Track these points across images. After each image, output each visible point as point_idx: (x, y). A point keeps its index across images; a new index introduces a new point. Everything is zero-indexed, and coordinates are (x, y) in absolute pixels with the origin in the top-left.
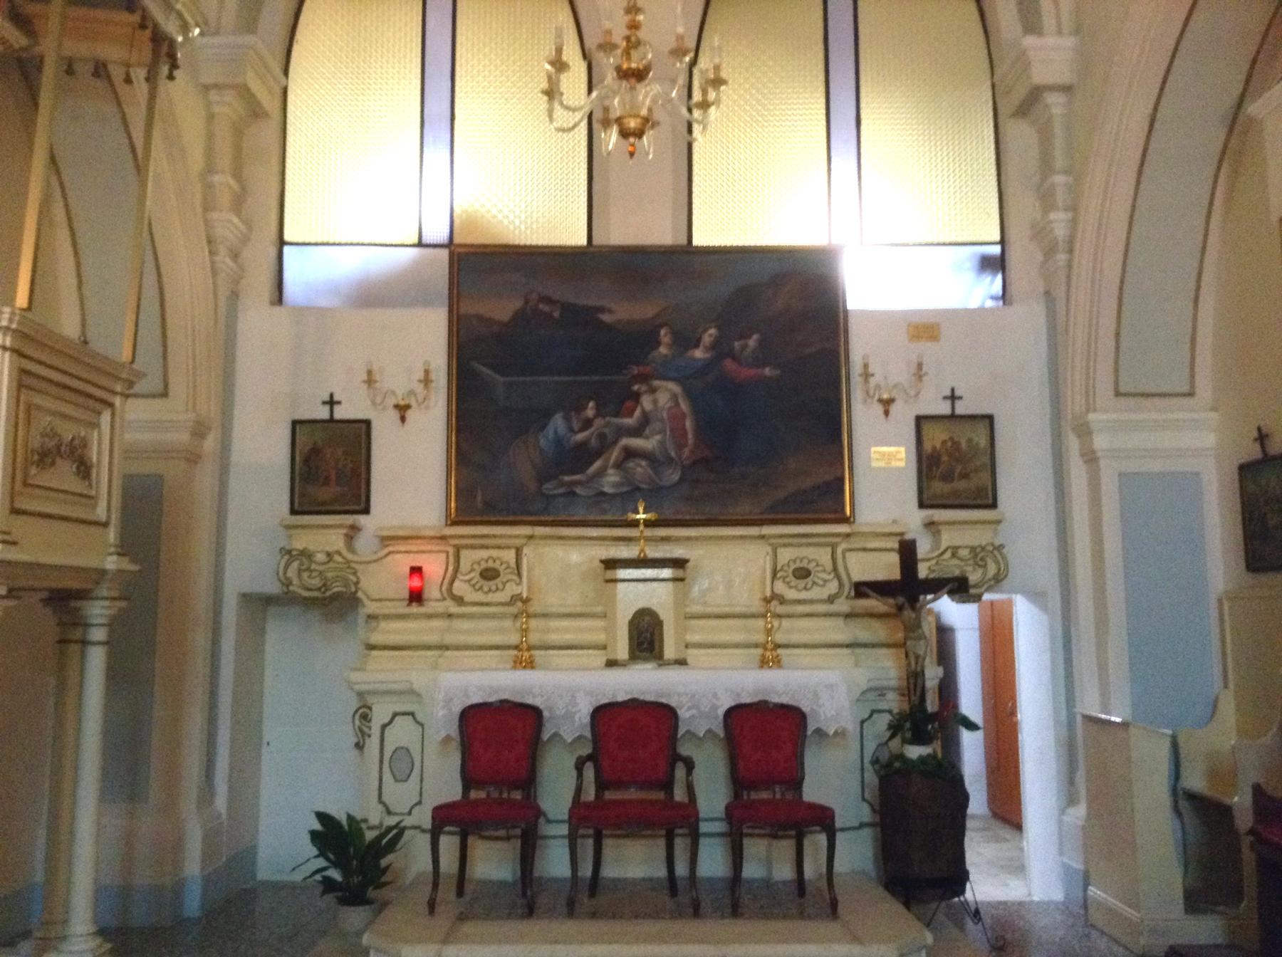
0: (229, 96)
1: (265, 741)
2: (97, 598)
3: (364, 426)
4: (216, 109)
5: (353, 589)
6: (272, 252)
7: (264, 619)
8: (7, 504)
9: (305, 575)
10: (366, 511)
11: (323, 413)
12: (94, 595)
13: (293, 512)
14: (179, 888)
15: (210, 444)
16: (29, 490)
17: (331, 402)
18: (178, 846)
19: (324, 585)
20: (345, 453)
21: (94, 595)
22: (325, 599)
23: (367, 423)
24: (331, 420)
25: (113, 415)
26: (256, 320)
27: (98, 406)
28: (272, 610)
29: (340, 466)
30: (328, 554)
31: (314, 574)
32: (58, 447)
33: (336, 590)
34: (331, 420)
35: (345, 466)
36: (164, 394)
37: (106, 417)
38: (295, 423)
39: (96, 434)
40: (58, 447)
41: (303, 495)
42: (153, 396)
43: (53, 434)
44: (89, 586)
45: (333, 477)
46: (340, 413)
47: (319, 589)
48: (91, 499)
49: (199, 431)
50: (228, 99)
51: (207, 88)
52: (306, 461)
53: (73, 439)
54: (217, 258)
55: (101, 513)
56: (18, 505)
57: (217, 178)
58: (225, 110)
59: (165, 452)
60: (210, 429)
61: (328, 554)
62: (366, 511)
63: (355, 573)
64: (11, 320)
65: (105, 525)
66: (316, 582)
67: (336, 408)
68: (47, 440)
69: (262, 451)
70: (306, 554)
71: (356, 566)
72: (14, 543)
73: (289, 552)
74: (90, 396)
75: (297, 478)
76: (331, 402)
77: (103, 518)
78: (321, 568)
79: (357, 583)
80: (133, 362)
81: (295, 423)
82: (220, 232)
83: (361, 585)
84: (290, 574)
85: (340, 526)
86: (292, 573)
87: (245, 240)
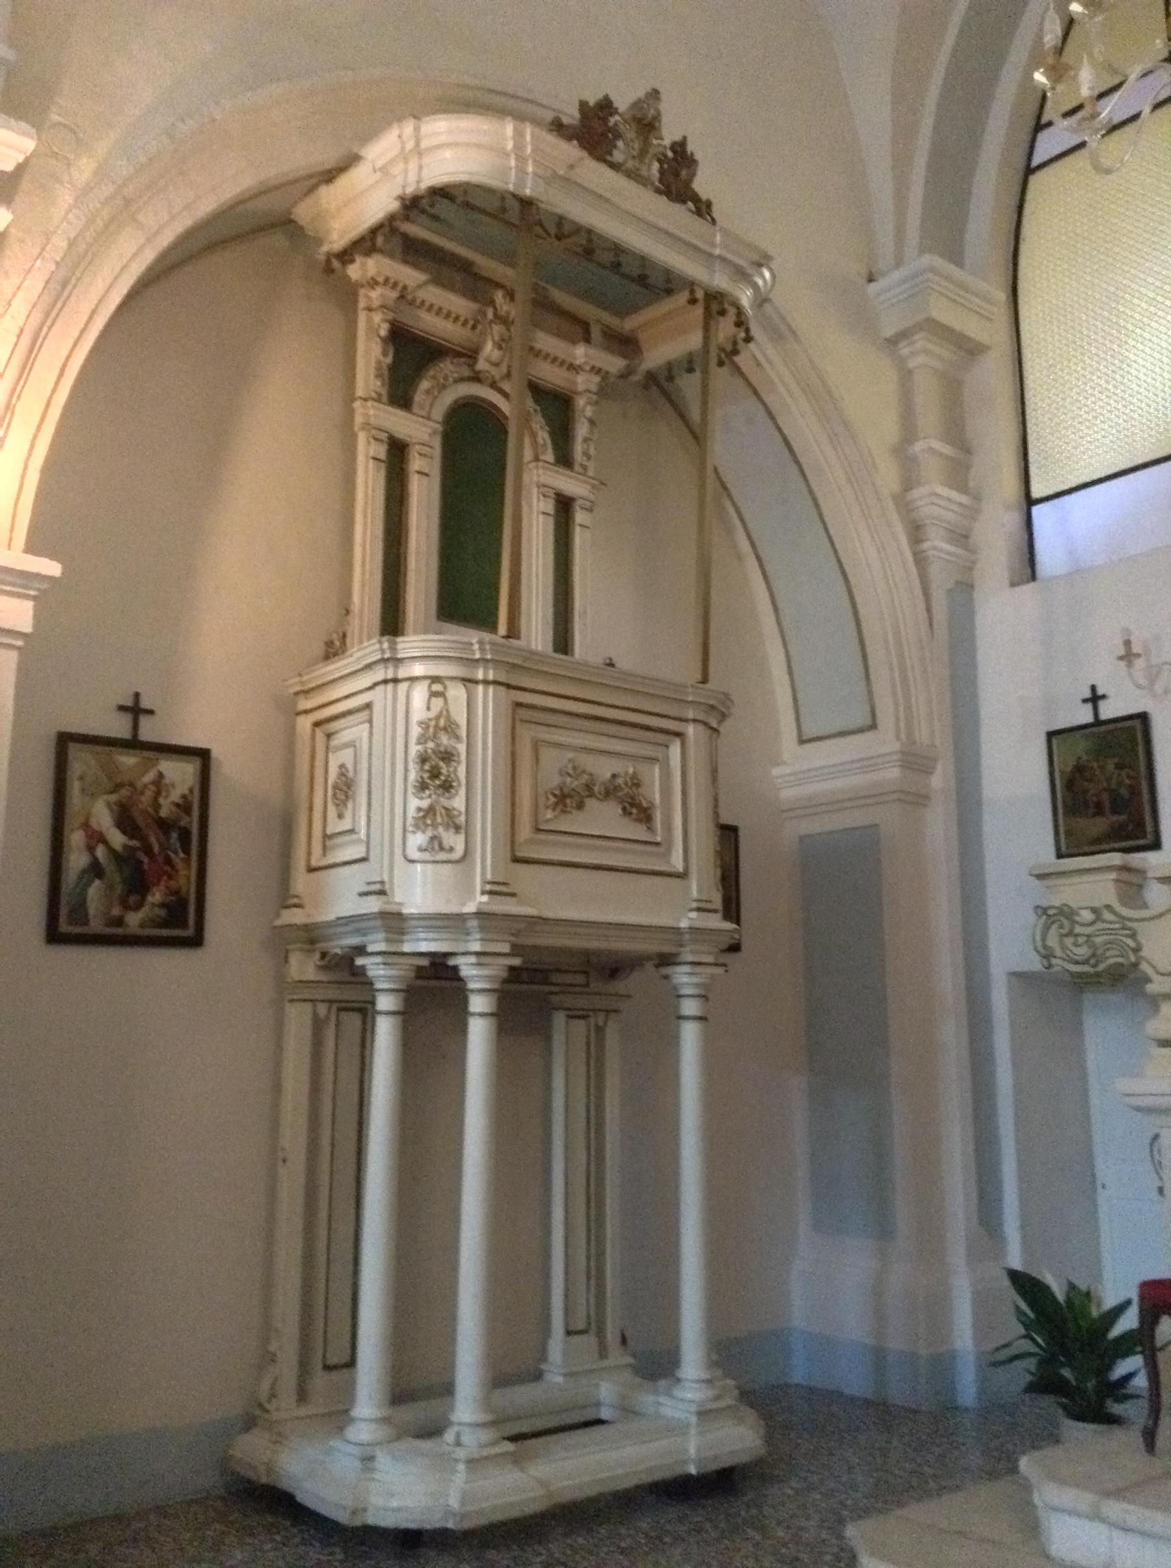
0: (921, 341)
1: (1099, 1183)
2: (680, 964)
3: (1137, 723)
4: (911, 364)
5: (1133, 959)
6: (1014, 519)
7: (1078, 1011)
8: (509, 855)
9: (1069, 941)
10: (1156, 845)
11: (1085, 715)
12: (680, 960)
13: (1060, 856)
14: (942, 1365)
15: (939, 780)
16: (542, 836)
17: (1095, 698)
18: (937, 1307)
19: (1094, 955)
20: (1119, 767)
21: (680, 960)
22: (1097, 975)
23: (1143, 718)
24: (1098, 722)
25: (683, 745)
26: (1002, 613)
27: (661, 738)
28: (1088, 999)
29: (1113, 786)
30: (1094, 910)
31: (1081, 940)
32: (589, 787)
33: (1112, 961)
34: (1098, 722)
35: (1120, 784)
36: (873, 726)
37: (675, 750)
38: (1051, 735)
39: (657, 770)
40: (589, 787)
41: (1069, 833)
42: (861, 730)
43: (577, 771)
44: (674, 950)
45: (1107, 804)
46: (1108, 711)
47: (1086, 962)
48: (661, 847)
49: (916, 762)
50: (919, 345)
51: (893, 342)
52: (1070, 784)
53: (614, 776)
54: (926, 545)
55: (677, 862)
56: (519, 854)
57: (918, 447)
58: (921, 359)
59: (873, 797)
60: (935, 760)
61: (1094, 910)
62: (1156, 845)
63: (1133, 936)
64: (482, 650)
65: (683, 876)
66: (1083, 951)
67: (1102, 705)
68: (569, 780)
69: (1017, 781)
70: (1066, 913)
71: (1134, 925)
72: (513, 895)
73: (1045, 910)
74: (648, 728)
75: (1060, 811)
76: (1095, 698)
77: (680, 867)
78: (1088, 930)
79: (1137, 950)
80: (705, 680)
81: (1051, 735)
82: (927, 510)
83: (1144, 953)
84: (1050, 943)
85: (1110, 868)
86: (1053, 941)
87: (973, 512)
